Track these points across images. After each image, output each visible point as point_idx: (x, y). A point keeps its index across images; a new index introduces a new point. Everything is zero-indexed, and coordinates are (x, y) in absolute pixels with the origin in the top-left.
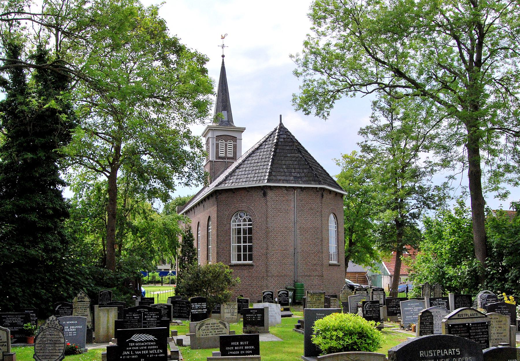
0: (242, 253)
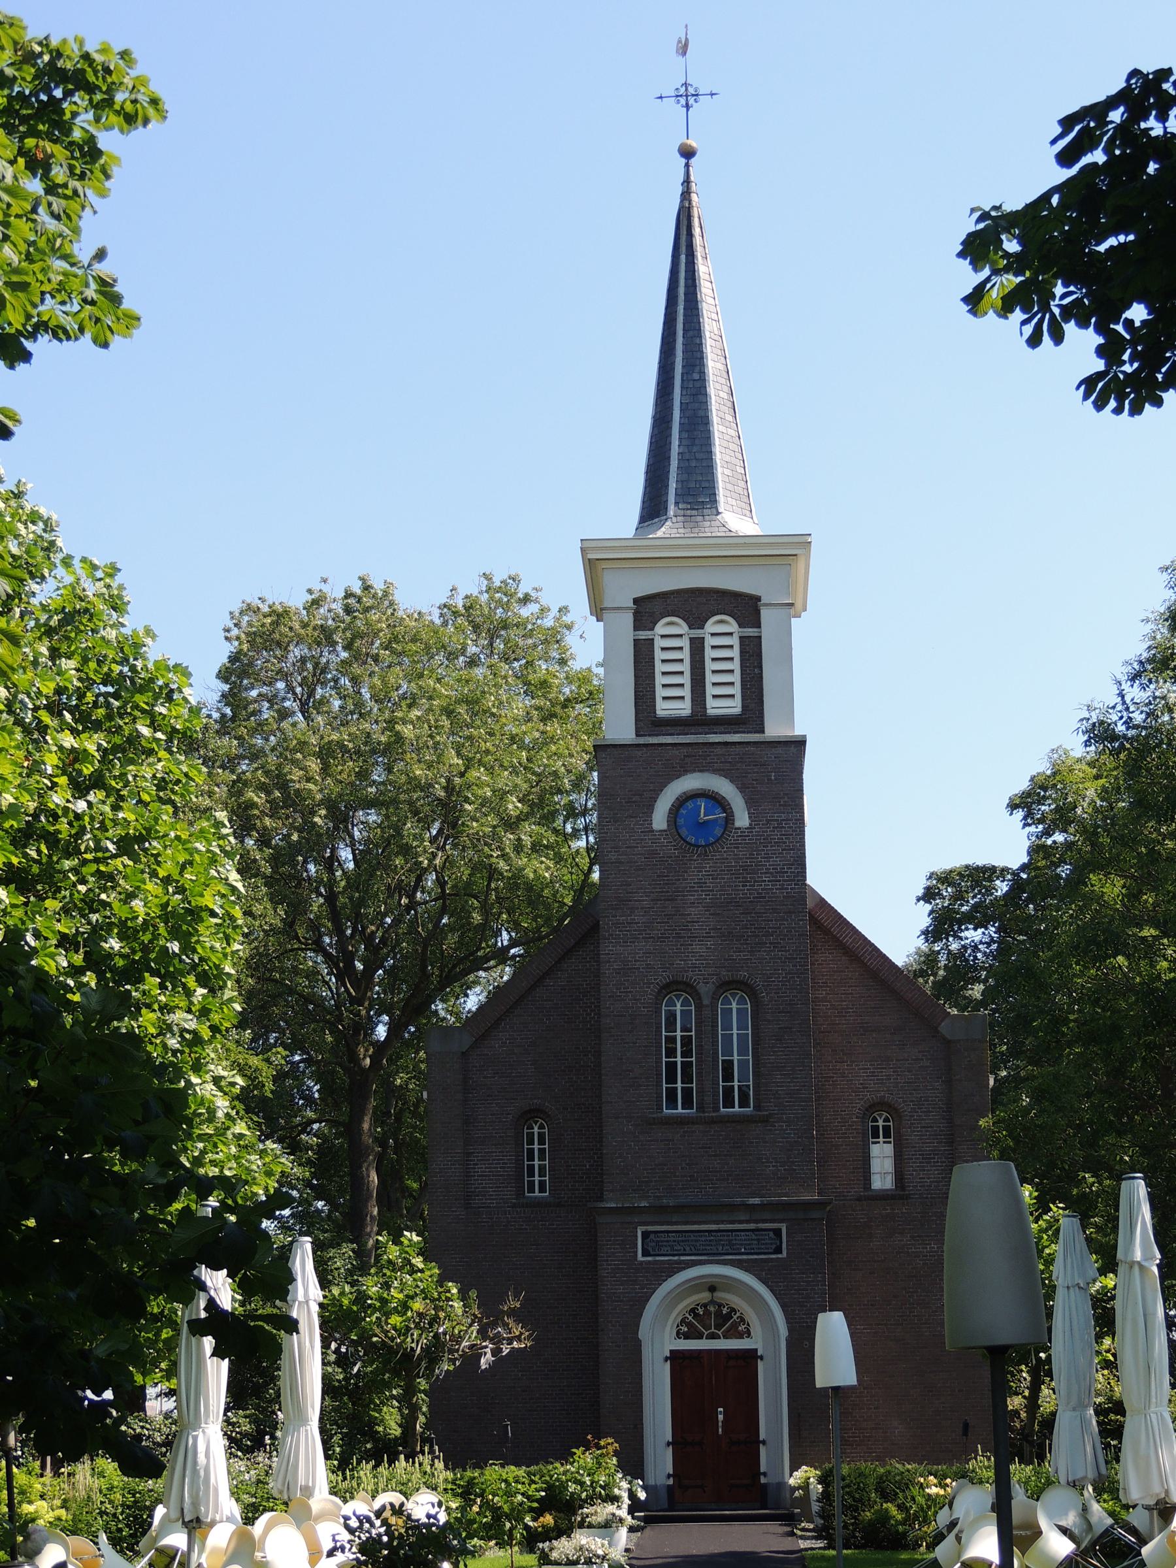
0: (735, 1031)
